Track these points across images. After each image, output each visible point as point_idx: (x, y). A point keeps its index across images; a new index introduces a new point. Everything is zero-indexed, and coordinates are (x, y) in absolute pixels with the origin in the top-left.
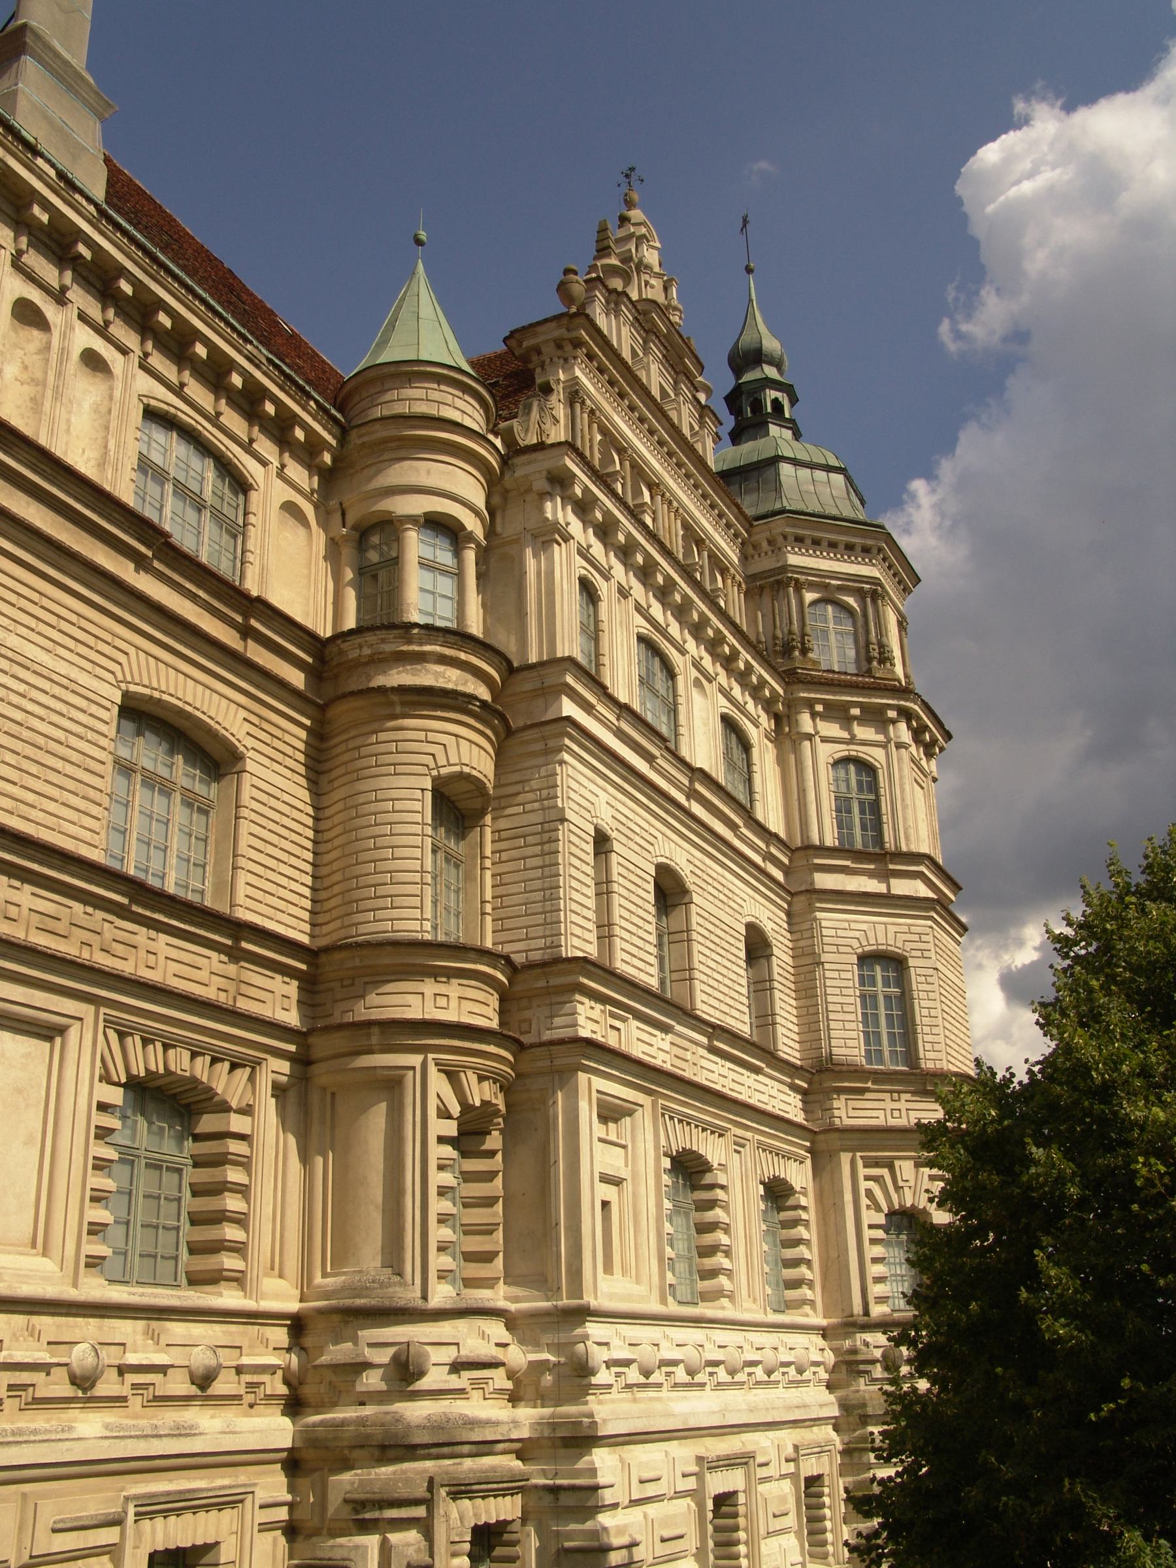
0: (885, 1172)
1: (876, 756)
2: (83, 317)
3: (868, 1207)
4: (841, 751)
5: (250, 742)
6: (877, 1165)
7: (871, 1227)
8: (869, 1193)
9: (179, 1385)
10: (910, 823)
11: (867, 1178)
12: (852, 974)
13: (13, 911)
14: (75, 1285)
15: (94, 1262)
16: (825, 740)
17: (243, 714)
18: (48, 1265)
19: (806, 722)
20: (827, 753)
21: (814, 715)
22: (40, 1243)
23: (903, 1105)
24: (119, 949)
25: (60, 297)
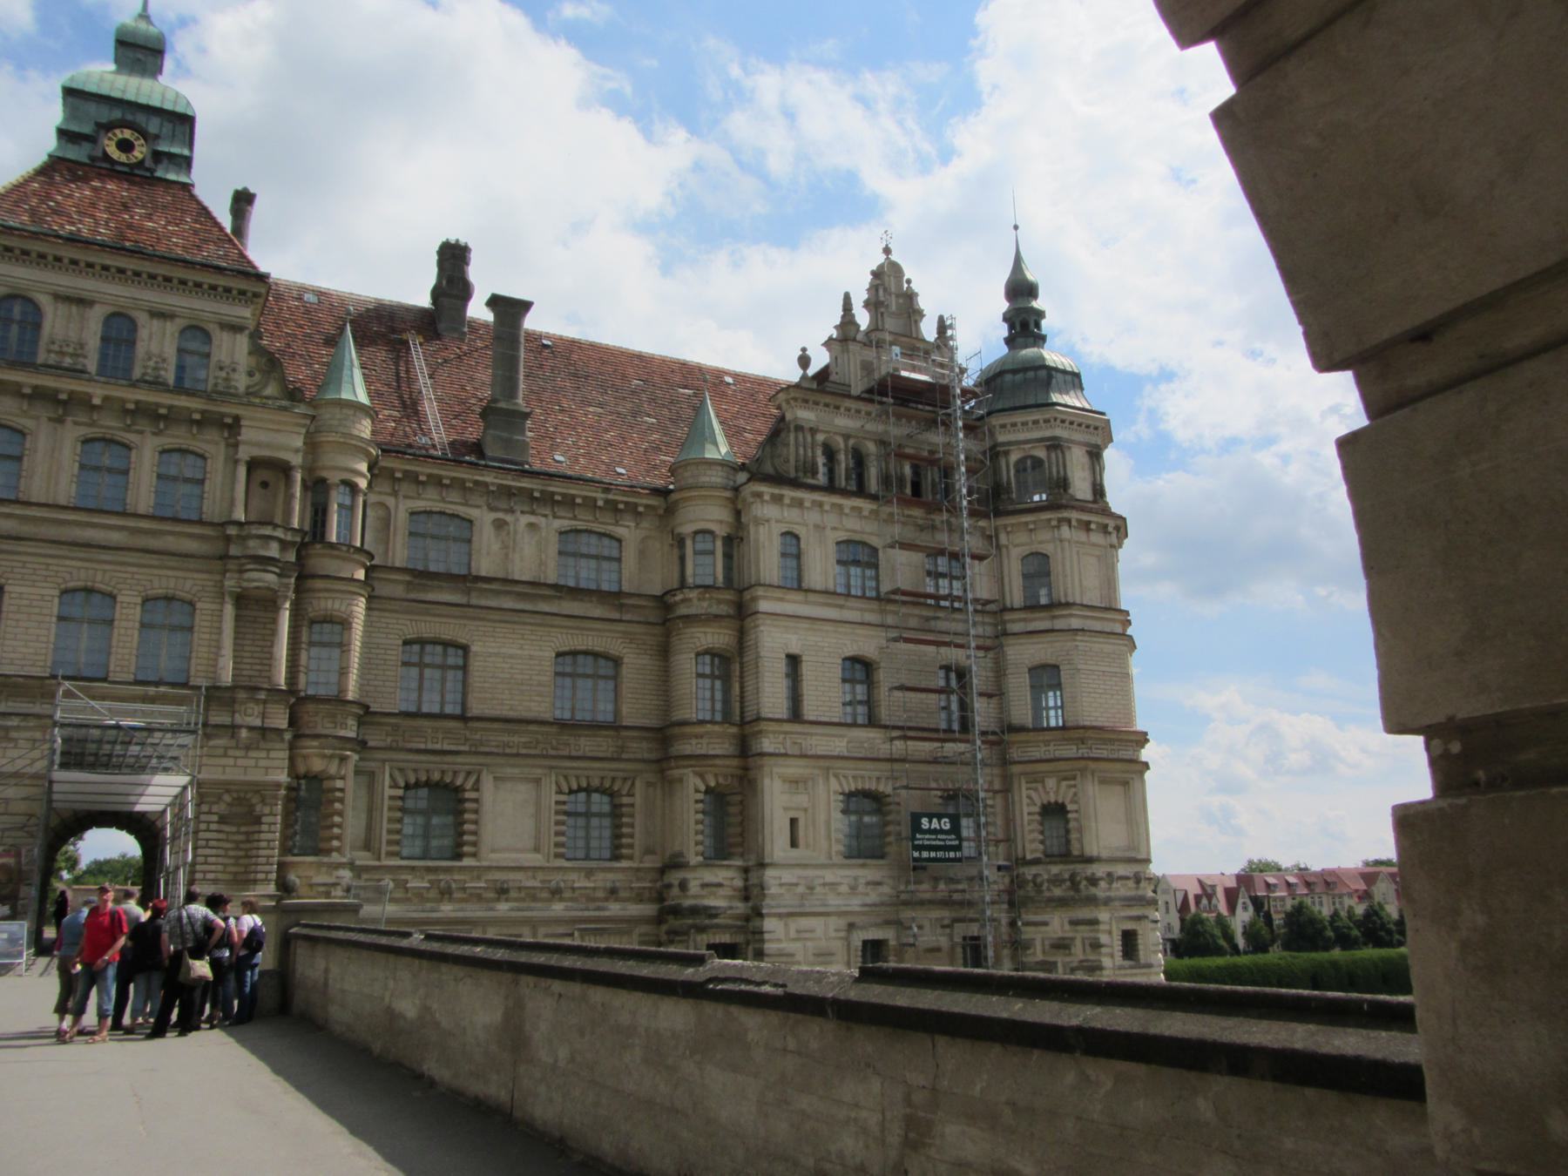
0: (1039, 786)
1: (1047, 549)
2: (522, 512)
3: (1028, 805)
4: (1026, 550)
5: (625, 651)
6: (1036, 781)
7: (1029, 814)
8: (1029, 797)
9: (600, 894)
10: (1069, 585)
11: (1027, 789)
12: (1026, 678)
13: (511, 744)
14: (548, 861)
15: (557, 856)
16: (1016, 546)
17: (620, 641)
18: (539, 856)
19: (1003, 539)
20: (1016, 553)
21: (1008, 533)
22: (537, 850)
23: (1051, 748)
24: (562, 747)
25: (512, 511)
